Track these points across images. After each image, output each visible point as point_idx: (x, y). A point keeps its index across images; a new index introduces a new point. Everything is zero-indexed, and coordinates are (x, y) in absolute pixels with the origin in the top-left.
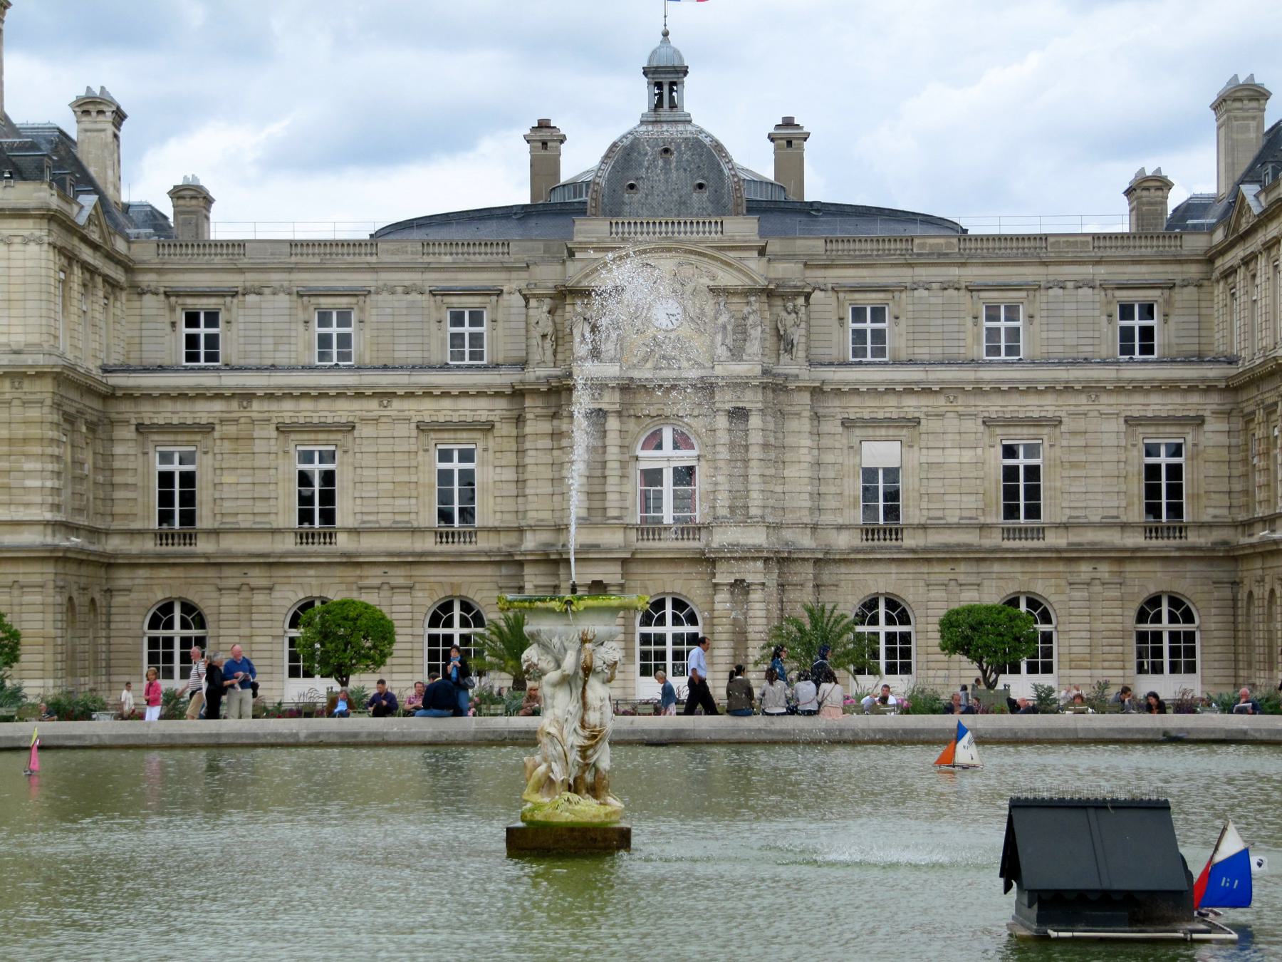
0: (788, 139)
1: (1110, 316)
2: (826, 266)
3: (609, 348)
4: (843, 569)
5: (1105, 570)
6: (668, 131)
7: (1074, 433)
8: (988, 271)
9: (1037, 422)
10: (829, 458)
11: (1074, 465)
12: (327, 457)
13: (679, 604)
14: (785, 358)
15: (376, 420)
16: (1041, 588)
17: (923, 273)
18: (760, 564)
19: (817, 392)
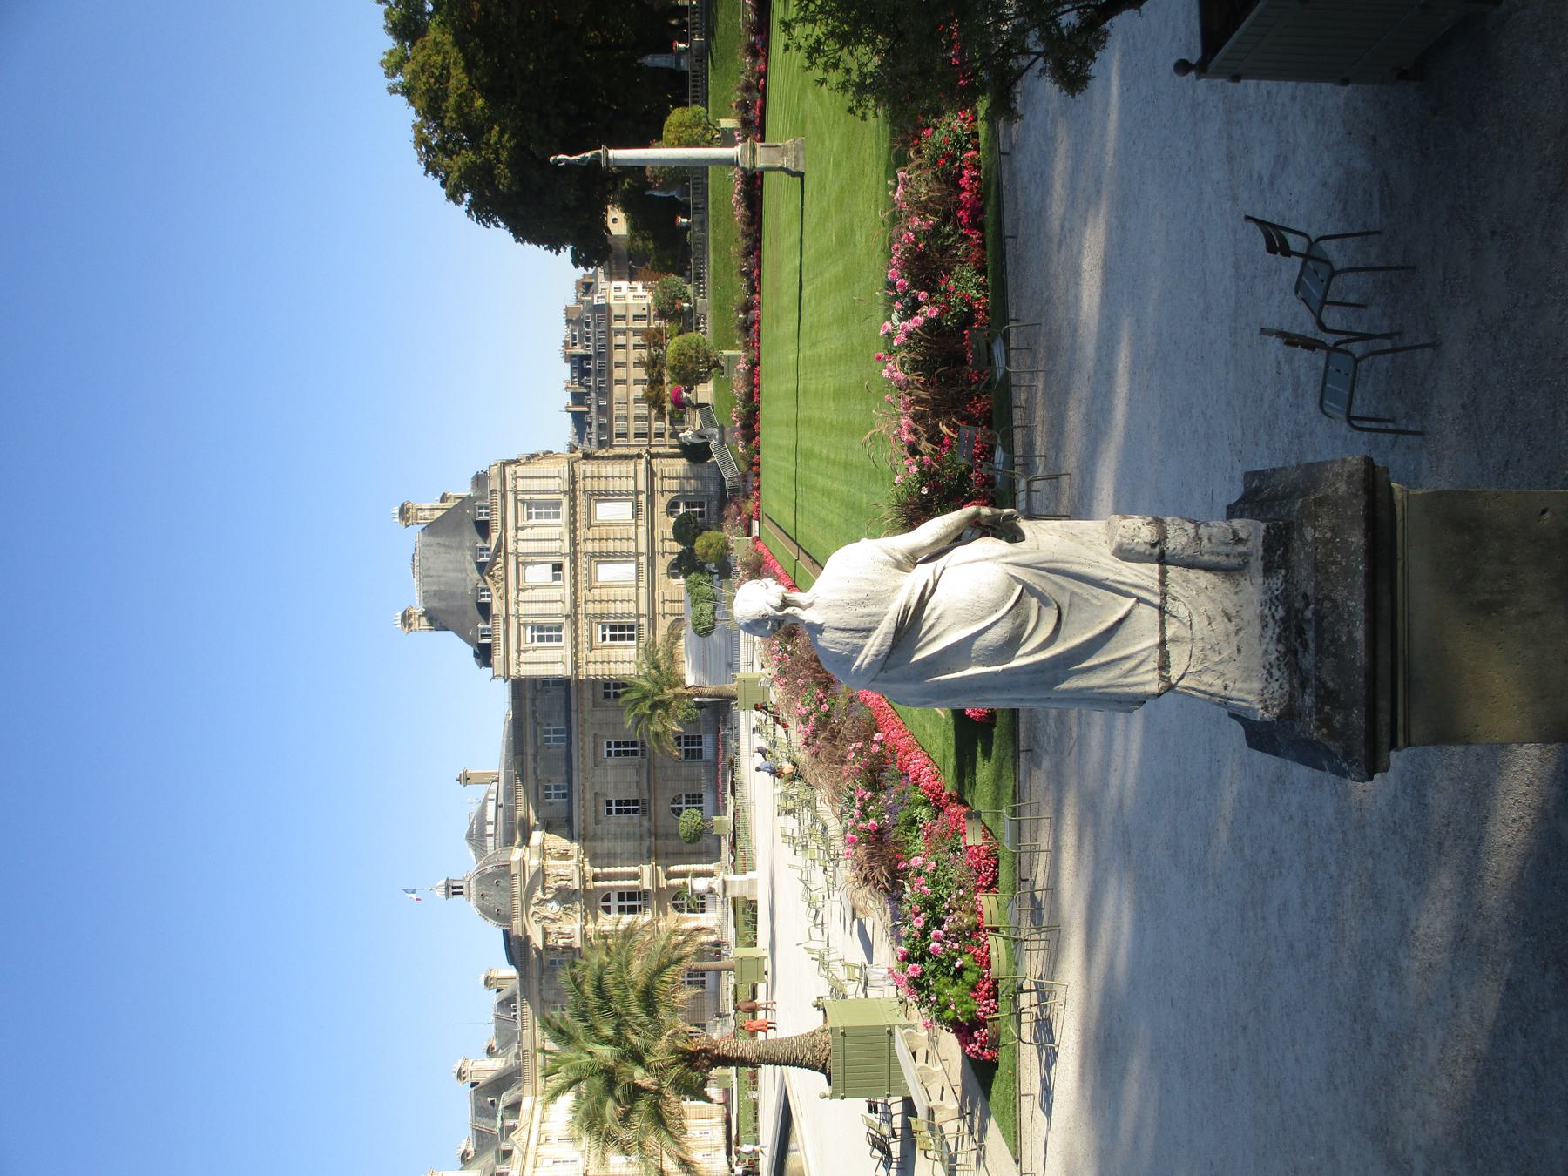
0: (466, 779)
3: (566, 929)
6: (473, 890)
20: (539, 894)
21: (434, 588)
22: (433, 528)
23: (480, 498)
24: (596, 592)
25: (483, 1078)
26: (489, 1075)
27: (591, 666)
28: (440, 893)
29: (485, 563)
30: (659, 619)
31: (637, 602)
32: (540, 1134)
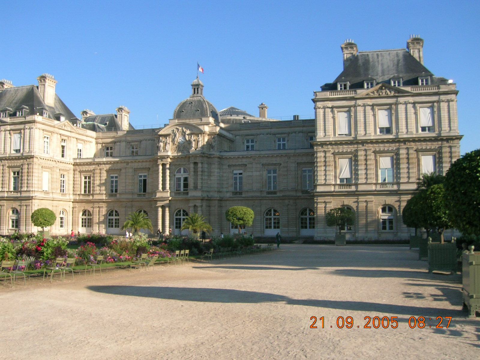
1: (307, 139)
2: (239, 130)
4: (228, 202)
5: (291, 201)
7: (284, 167)
8: (277, 130)
9: (275, 164)
10: (225, 175)
11: (284, 175)
12: (116, 177)
13: (184, 211)
14: (212, 150)
15: (126, 168)
16: (276, 207)
17: (262, 131)
18: (200, 201)
19: (220, 158)
20: (188, 132)
21: (371, 60)
22: (408, 58)
23: (432, 81)
24: (372, 157)
25: (118, 120)
26: (120, 123)
27: (322, 154)
28: (195, 81)
29: (390, 83)
30: (354, 199)
31: (366, 184)
32: (68, 137)
